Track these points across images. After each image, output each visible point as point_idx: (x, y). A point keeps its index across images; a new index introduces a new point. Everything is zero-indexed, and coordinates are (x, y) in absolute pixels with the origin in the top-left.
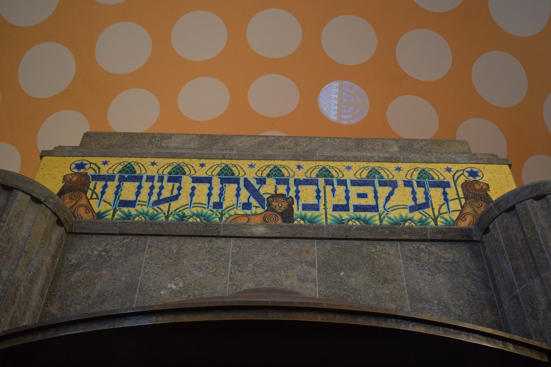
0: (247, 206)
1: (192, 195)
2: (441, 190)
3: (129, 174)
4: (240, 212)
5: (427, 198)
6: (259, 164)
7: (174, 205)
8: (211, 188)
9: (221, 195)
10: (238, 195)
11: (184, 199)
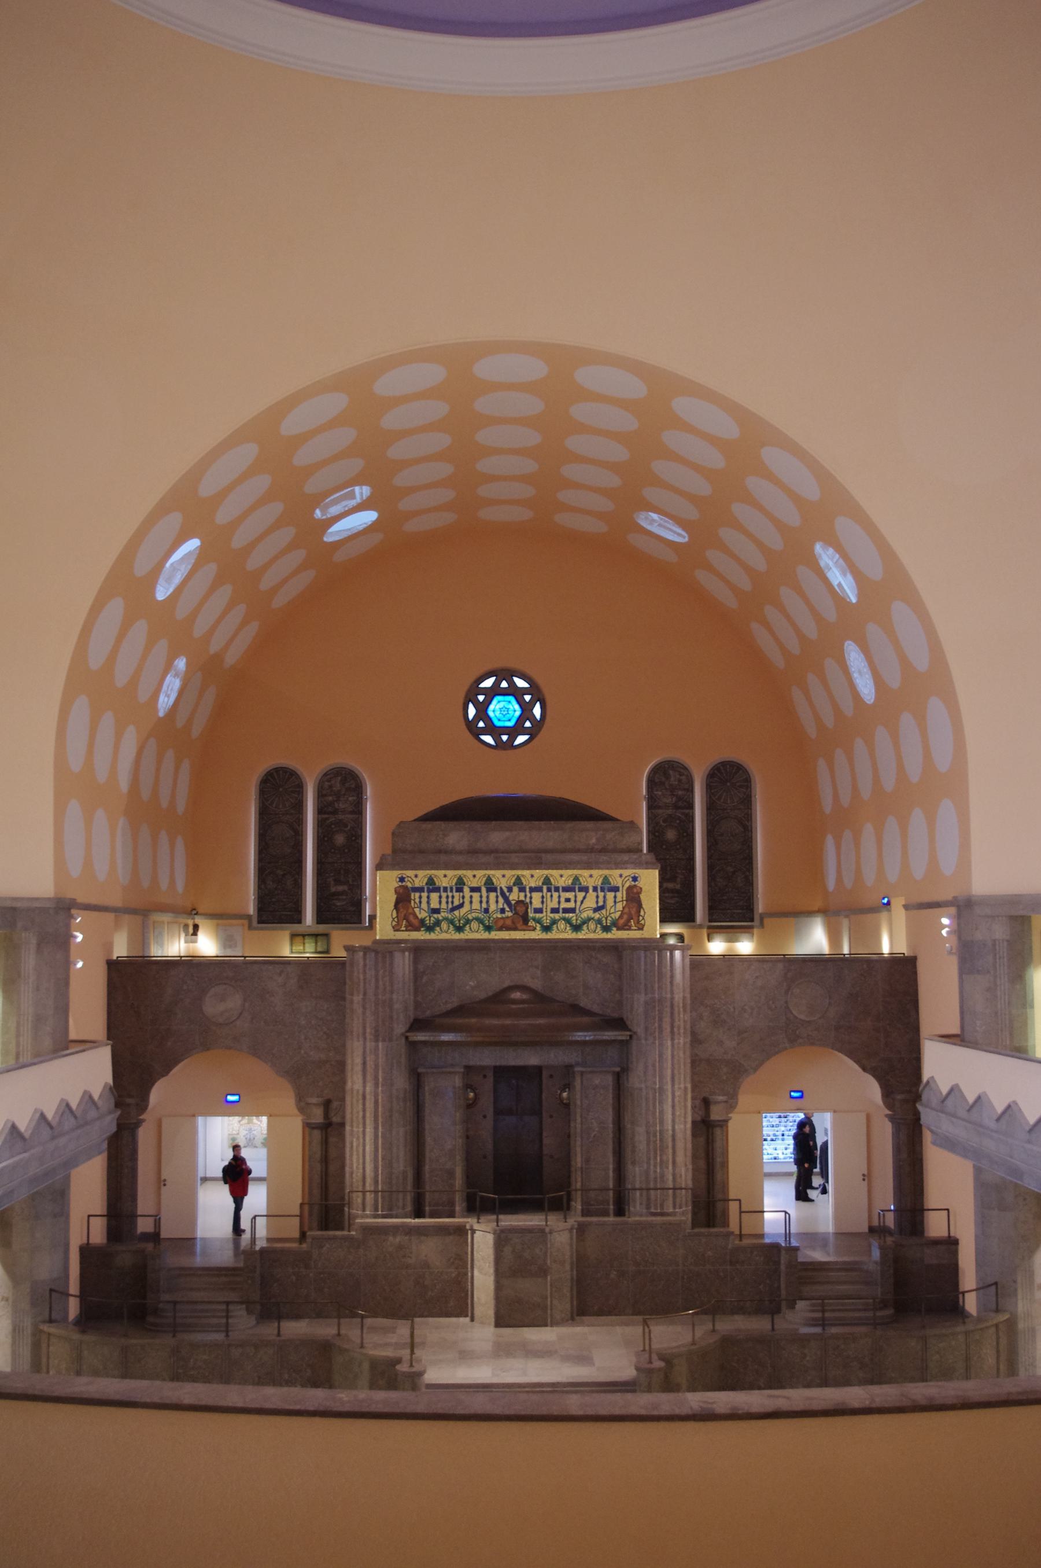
0: (503, 911)
1: (471, 902)
2: (613, 894)
3: (432, 886)
4: (499, 916)
5: (604, 902)
6: (509, 873)
7: (463, 911)
8: (481, 897)
9: (488, 902)
10: (497, 902)
11: (466, 907)
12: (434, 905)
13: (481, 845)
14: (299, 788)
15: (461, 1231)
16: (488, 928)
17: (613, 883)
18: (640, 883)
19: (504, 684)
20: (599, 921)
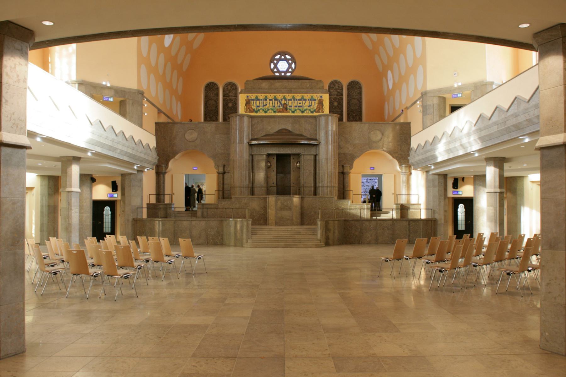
0: (279, 106)
3: (257, 99)
6: (281, 95)
7: (267, 107)
11: (268, 105)
12: (258, 104)
13: (273, 87)
14: (217, 89)
15: (265, 199)
16: (275, 112)
17: (314, 98)
18: (323, 98)
19: (283, 57)
20: (310, 110)
